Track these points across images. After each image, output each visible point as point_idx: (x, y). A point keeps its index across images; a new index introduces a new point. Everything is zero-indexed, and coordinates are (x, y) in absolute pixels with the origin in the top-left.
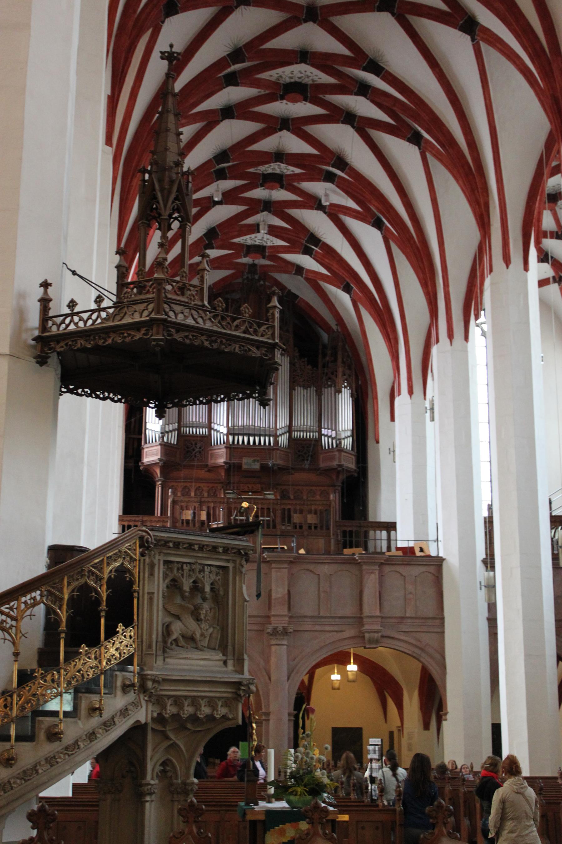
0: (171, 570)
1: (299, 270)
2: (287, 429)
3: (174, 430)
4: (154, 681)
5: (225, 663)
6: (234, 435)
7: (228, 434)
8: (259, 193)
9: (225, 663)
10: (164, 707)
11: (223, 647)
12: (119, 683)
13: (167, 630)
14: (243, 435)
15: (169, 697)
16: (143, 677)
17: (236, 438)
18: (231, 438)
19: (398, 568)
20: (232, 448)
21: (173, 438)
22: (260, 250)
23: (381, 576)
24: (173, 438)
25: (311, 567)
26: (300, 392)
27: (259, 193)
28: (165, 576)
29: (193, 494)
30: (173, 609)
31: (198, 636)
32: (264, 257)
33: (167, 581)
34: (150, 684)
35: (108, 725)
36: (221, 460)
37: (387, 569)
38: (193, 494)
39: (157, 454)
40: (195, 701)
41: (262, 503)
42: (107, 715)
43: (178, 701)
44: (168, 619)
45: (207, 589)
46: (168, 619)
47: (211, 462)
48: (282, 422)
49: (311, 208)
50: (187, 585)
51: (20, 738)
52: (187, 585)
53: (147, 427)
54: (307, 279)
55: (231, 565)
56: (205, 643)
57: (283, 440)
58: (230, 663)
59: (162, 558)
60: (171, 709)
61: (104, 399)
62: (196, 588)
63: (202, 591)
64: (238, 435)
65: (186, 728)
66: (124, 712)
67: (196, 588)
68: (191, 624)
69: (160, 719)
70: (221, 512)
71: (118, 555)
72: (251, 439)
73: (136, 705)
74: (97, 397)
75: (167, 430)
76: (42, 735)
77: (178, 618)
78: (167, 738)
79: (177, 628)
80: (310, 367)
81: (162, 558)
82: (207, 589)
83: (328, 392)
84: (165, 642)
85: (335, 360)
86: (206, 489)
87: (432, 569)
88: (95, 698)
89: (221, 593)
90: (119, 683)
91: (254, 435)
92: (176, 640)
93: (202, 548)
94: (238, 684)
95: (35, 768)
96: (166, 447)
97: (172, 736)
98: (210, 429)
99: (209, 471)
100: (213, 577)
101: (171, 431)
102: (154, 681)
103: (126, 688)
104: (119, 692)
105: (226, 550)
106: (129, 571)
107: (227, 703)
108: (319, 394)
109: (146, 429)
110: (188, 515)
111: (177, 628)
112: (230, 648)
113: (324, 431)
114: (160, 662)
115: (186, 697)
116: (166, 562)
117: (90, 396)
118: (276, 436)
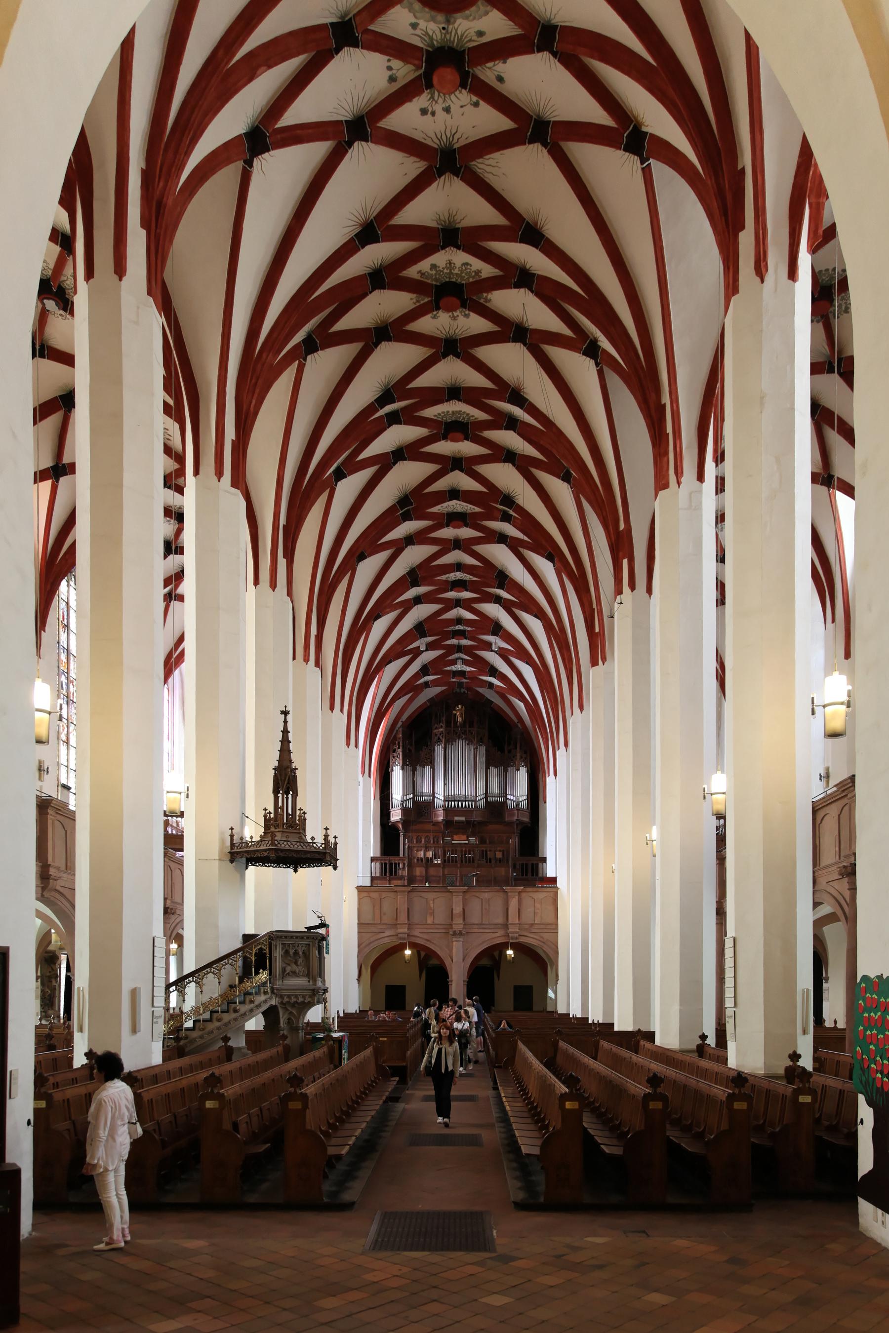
0: (285, 946)
1: (491, 685)
2: (483, 796)
3: (410, 799)
4: (277, 990)
5: (309, 981)
6: (448, 801)
7: (445, 801)
9: (309, 981)
10: (283, 999)
11: (308, 975)
12: (262, 991)
13: (284, 970)
14: (455, 801)
15: (285, 995)
16: (272, 989)
17: (450, 803)
18: (447, 803)
20: (447, 810)
21: (410, 805)
22: (462, 673)
24: (410, 805)
26: (492, 770)
28: (282, 949)
29: (423, 840)
30: (287, 962)
31: (297, 971)
32: (465, 678)
33: (284, 951)
34: (275, 991)
35: (259, 1006)
36: (441, 818)
38: (423, 840)
39: (399, 816)
40: (296, 996)
41: (465, 847)
42: (257, 1003)
43: (289, 996)
44: (285, 965)
45: (301, 953)
46: (285, 965)
47: (434, 819)
48: (481, 791)
49: (488, 650)
50: (292, 952)
51: (222, 1012)
52: (292, 952)
53: (393, 796)
54: (496, 692)
55: (311, 943)
56: (301, 974)
57: (482, 804)
58: (311, 982)
59: (281, 942)
60: (286, 999)
61: (269, 866)
62: (296, 953)
63: (299, 953)
64: (451, 801)
65: (295, 1007)
66: (265, 1002)
67: (296, 953)
68: (294, 967)
69: (282, 1003)
70: (440, 852)
71: (259, 944)
72: (460, 803)
73: (271, 998)
74: (266, 866)
75: (405, 799)
76: (231, 1011)
77: (289, 965)
78: (288, 1010)
79: (288, 969)
80: (499, 753)
81: (281, 942)
82: (301, 953)
84: (283, 975)
85: (516, 748)
86: (432, 837)
88: (252, 997)
89: (308, 954)
90: (262, 991)
91: (462, 801)
92: (288, 973)
93: (297, 938)
94: (313, 990)
95: (229, 1022)
96: (405, 811)
97: (290, 1009)
98: (434, 797)
99: (433, 825)
100: (304, 948)
101: (406, 801)
102: (277, 990)
103: (265, 993)
104: (262, 995)
105: (308, 938)
106: (265, 950)
107: (310, 996)
109: (392, 798)
110: (421, 854)
111: (288, 969)
112: (311, 976)
114: (281, 981)
115: (293, 995)
116: (282, 944)
117: (262, 866)
118: (476, 801)
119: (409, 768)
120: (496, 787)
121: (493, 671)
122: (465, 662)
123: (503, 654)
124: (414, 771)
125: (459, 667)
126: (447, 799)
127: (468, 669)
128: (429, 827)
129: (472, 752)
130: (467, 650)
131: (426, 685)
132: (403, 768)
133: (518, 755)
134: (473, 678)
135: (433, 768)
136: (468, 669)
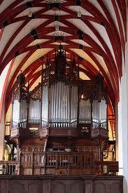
6: (51, 123)
8: (51, 12)
19: (103, 182)
20: (50, 129)
22: (60, 39)
23: (94, 185)
25: (62, 181)
27: (51, 12)
37: (96, 182)
83: (95, 102)
87: (118, 182)
96: (21, 129)
108: (91, 102)
113: (94, 120)
118: (70, 123)
119: (25, 101)
120: (85, 115)
121: (81, 35)
122: (61, 28)
123: (85, 20)
124: (28, 102)
125: (59, 33)
126: (50, 122)
127: (66, 34)
128: (38, 141)
129: (68, 90)
130: (62, 19)
131: (38, 47)
132: (20, 101)
133: (100, 93)
134: (66, 39)
135: (41, 100)
136: (66, 34)
